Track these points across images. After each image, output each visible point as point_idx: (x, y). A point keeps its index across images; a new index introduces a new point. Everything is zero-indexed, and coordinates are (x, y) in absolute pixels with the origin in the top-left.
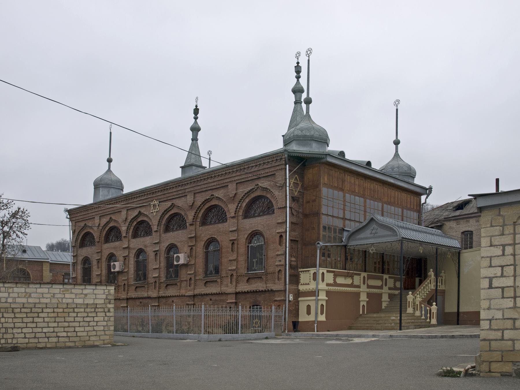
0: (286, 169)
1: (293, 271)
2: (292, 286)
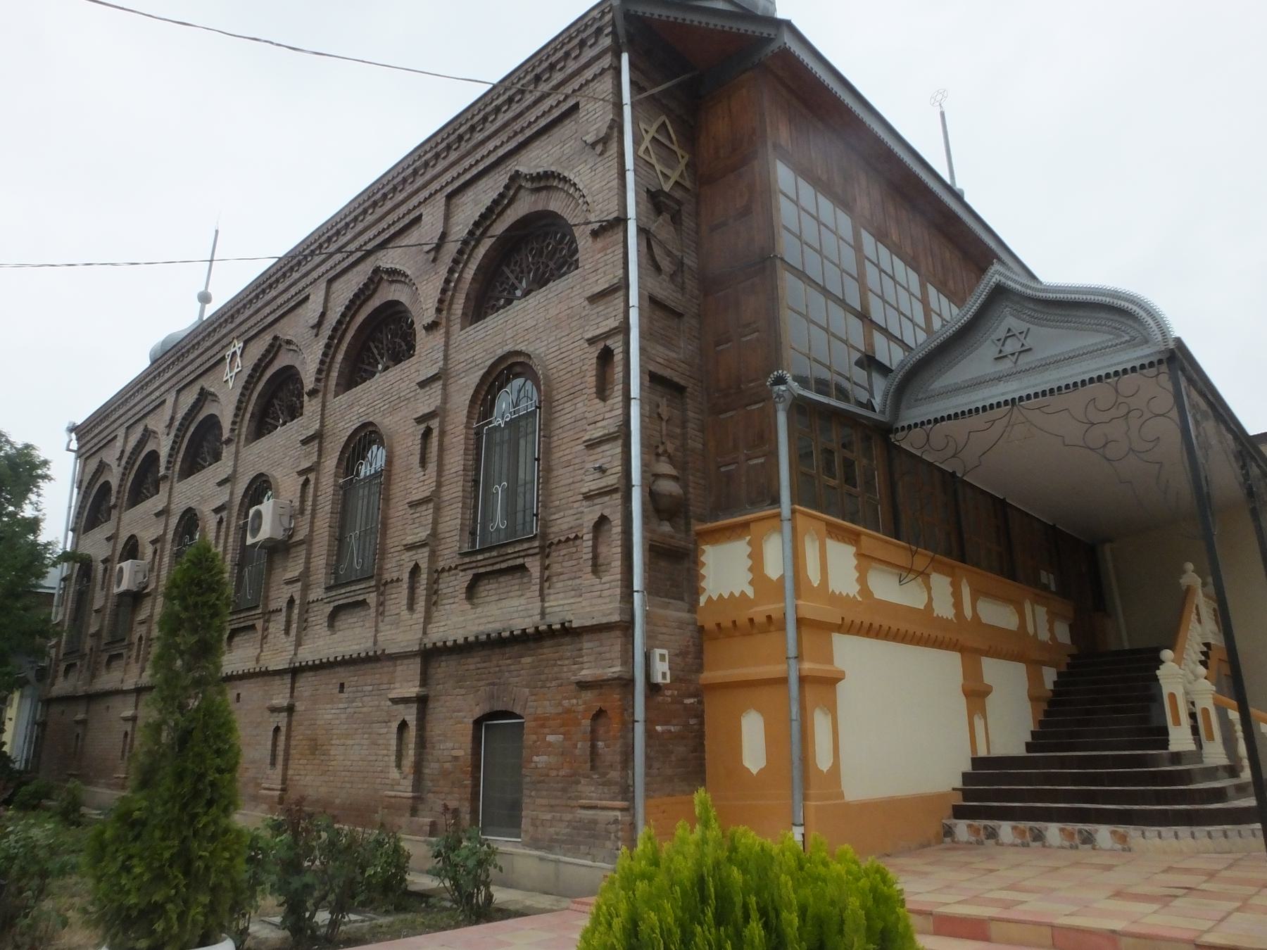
1: (666, 528)
2: (666, 606)
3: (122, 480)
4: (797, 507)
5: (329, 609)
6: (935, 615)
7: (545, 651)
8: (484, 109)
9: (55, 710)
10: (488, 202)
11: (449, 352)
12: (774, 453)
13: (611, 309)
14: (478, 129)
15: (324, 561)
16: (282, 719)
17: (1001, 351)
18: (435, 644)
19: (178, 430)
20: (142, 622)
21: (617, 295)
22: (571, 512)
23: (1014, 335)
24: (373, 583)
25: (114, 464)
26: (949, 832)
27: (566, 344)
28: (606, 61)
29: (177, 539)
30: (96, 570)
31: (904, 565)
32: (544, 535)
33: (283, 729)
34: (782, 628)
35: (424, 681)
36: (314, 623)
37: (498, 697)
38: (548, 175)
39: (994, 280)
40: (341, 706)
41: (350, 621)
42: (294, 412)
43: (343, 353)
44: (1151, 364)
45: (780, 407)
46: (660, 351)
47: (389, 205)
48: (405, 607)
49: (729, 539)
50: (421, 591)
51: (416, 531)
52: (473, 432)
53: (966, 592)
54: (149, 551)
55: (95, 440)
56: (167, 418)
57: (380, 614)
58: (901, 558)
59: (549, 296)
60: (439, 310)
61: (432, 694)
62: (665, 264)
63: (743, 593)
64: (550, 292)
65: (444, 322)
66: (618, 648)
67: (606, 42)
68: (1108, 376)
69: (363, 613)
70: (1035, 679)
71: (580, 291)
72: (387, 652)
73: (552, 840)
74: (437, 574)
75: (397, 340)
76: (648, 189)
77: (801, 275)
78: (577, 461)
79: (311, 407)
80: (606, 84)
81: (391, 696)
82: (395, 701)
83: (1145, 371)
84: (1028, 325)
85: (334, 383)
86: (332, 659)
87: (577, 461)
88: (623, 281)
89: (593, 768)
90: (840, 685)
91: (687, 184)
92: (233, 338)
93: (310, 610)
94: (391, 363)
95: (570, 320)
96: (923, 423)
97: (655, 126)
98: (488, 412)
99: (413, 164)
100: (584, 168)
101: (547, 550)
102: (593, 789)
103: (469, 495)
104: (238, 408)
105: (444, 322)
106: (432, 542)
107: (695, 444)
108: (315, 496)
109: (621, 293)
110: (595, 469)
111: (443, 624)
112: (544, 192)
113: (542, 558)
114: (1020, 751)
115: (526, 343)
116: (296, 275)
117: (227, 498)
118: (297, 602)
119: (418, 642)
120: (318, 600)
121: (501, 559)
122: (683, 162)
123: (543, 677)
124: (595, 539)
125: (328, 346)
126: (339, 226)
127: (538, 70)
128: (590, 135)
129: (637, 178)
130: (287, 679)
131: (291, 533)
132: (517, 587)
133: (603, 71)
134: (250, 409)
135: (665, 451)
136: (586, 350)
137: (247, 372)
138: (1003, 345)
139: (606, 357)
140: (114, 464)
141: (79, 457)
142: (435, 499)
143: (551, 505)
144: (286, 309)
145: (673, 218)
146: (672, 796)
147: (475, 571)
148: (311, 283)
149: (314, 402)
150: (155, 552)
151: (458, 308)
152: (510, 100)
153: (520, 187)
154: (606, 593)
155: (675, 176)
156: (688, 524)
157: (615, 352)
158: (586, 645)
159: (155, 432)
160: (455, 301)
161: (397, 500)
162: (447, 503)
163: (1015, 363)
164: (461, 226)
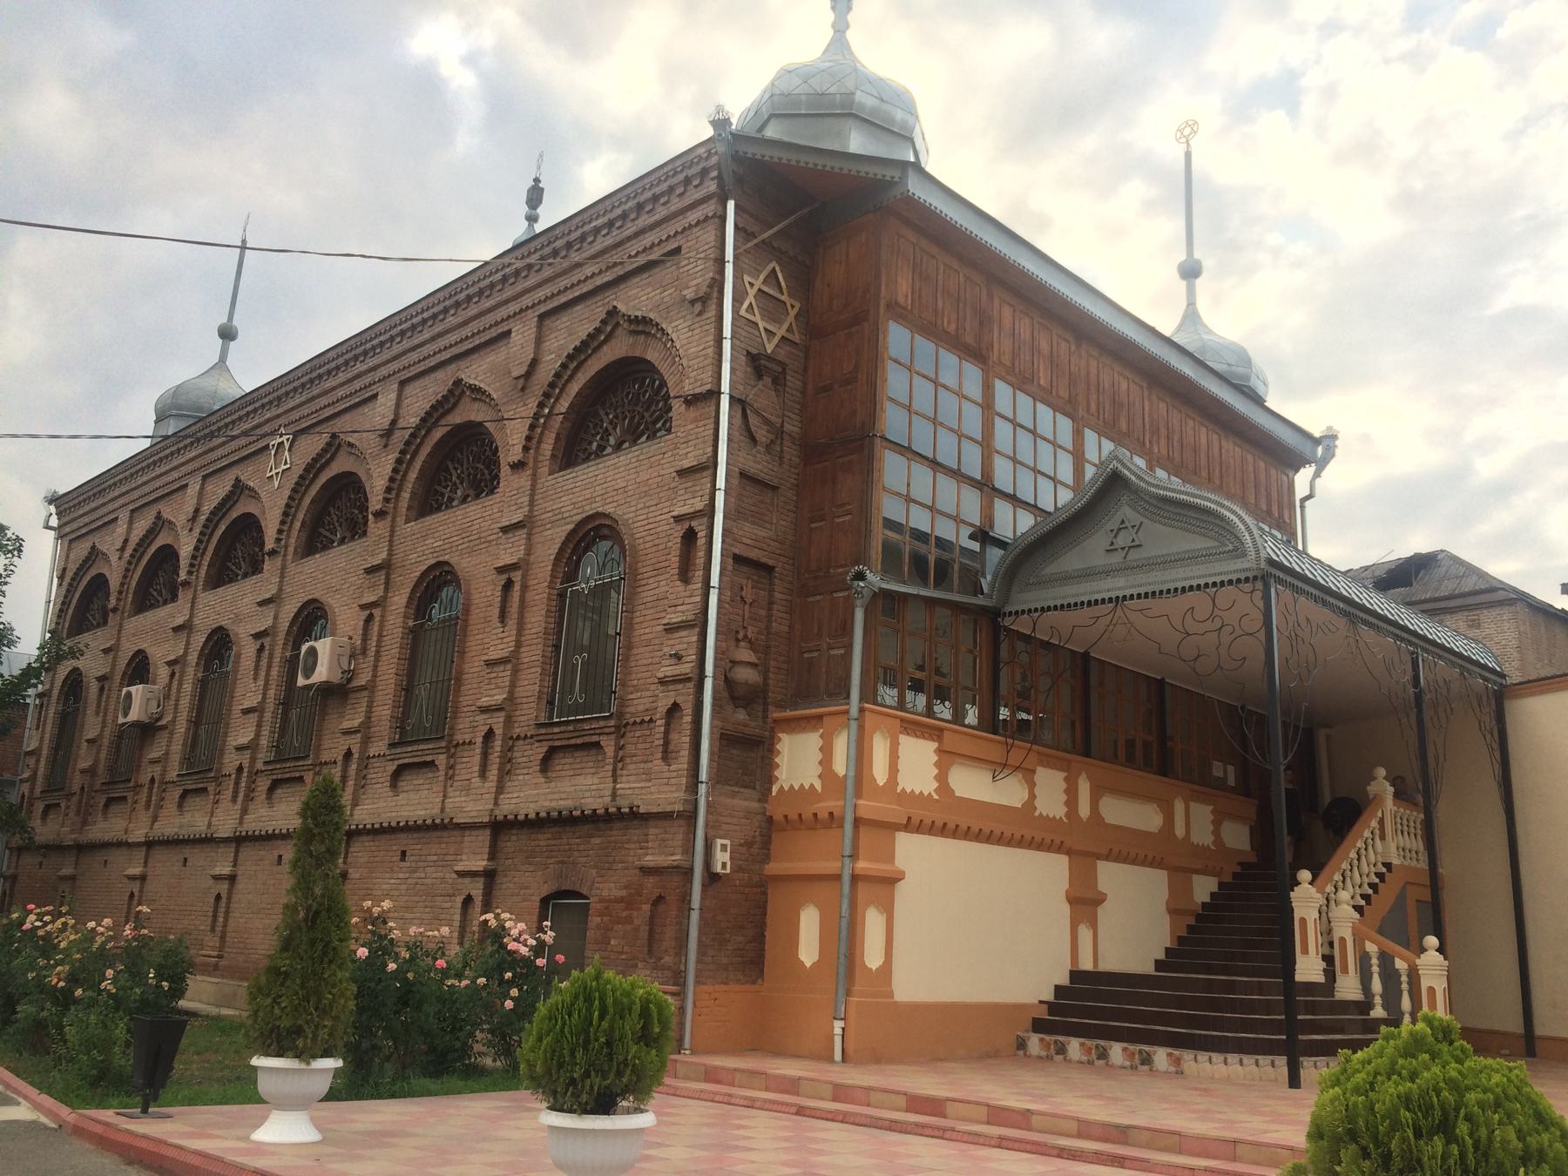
0: (723, 219)
1: (741, 715)
2: (734, 795)
3: (125, 577)
4: (866, 705)
5: (392, 767)
6: (1037, 814)
7: (614, 833)
8: (582, 226)
9: (28, 860)
10: (583, 335)
11: (536, 497)
12: (849, 647)
13: (698, 488)
14: (575, 248)
15: (389, 712)
17: (1112, 544)
18: (505, 816)
19: (205, 526)
20: (154, 762)
21: (704, 474)
22: (648, 694)
23: (1126, 528)
25: (114, 558)
26: (1022, 1045)
27: (655, 514)
28: (710, 208)
29: (203, 662)
30: (88, 688)
31: (999, 761)
32: (620, 715)
34: (841, 826)
35: (492, 856)
36: (373, 781)
37: (567, 876)
38: (645, 321)
39: (1111, 466)
40: (401, 876)
41: (415, 782)
42: (357, 529)
43: (416, 471)
44: (1247, 580)
45: (858, 602)
46: (748, 530)
47: (473, 310)
48: (476, 774)
49: (804, 730)
50: (495, 758)
51: (491, 692)
52: (556, 592)
54: (163, 673)
55: (86, 519)
56: (191, 509)
57: (450, 778)
59: (641, 458)
60: (526, 449)
61: (500, 868)
62: (762, 434)
63: (812, 784)
64: (642, 453)
65: (531, 465)
66: (680, 837)
67: (712, 187)
68: (1206, 585)
69: (430, 775)
70: (1179, 889)
71: (672, 459)
72: (454, 821)
74: (511, 741)
75: (480, 466)
76: (748, 352)
77: (907, 451)
78: (657, 641)
79: (377, 529)
80: (709, 235)
81: (456, 868)
82: (461, 874)
83: (1240, 586)
84: (1142, 519)
85: (406, 505)
87: (657, 641)
88: (711, 459)
89: (650, 952)
90: (900, 886)
91: (796, 338)
92: (280, 426)
93: (370, 766)
94: (471, 492)
95: (659, 490)
96: (1030, 610)
97: (762, 277)
98: (571, 576)
99: (502, 269)
100: (682, 325)
101: (623, 730)
102: (648, 973)
103: (548, 661)
104: (285, 514)
105: (531, 465)
106: (508, 707)
108: (380, 636)
110: (671, 655)
111: (516, 795)
112: (642, 337)
113: (617, 739)
114: (1149, 969)
115: (615, 504)
116: (360, 367)
117: (269, 622)
118: (356, 756)
119: (488, 813)
120: (379, 755)
121: (577, 734)
122: (793, 313)
123: (611, 859)
124: (668, 725)
125: (399, 461)
126: (415, 321)
127: (641, 199)
128: (690, 290)
129: (738, 342)
131: (350, 675)
132: (591, 764)
133: (707, 219)
134: (301, 516)
135: (746, 636)
136: (672, 526)
137: (298, 471)
138: (1115, 537)
139: (690, 537)
140: (114, 558)
141: (60, 537)
142: (514, 661)
143: (630, 683)
144: (348, 404)
145: (775, 381)
146: (726, 984)
147: (551, 743)
148: (379, 381)
149: (380, 524)
150: (173, 675)
151: (547, 447)
152: (610, 224)
153: (618, 324)
154: (673, 781)
155: (781, 331)
156: (765, 711)
157: (699, 535)
158: (652, 831)
159: (170, 523)
160: (545, 439)
161: (474, 653)
162: (526, 666)
163: (1125, 558)
164: (553, 356)
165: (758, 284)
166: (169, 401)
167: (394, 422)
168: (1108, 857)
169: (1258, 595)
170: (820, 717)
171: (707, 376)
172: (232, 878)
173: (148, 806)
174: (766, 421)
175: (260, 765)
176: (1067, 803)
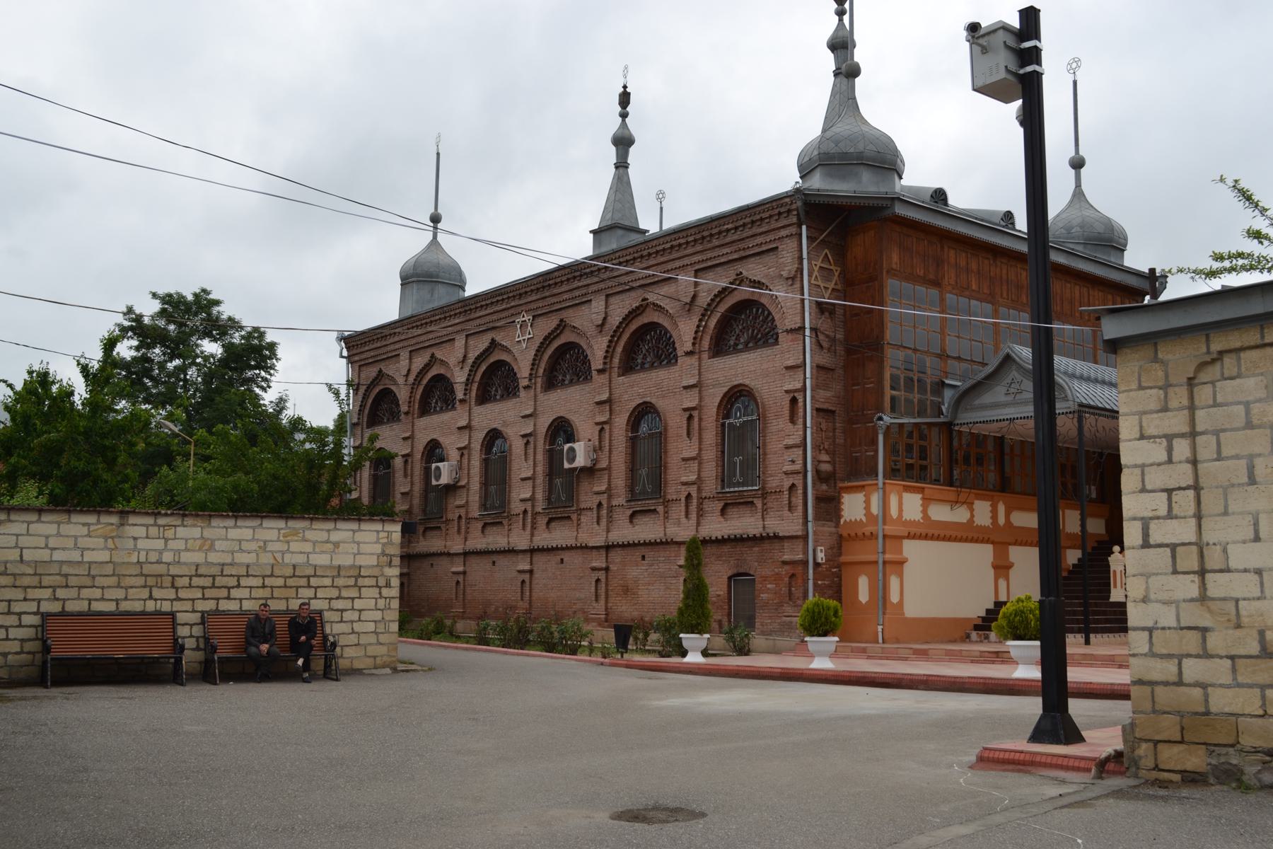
1: (824, 487)
2: (823, 525)
4: (887, 481)
12: (876, 451)
16: (602, 575)
24: (661, 500)
25: (401, 380)
26: (968, 636)
28: (793, 230)
32: (763, 488)
33: (603, 580)
34: (877, 538)
44: (1070, 412)
45: (880, 431)
46: (823, 394)
49: (855, 492)
53: (1001, 509)
55: (372, 354)
56: (461, 356)
57: (666, 518)
58: (952, 496)
60: (694, 344)
62: (825, 344)
66: (801, 547)
73: (771, 631)
79: (599, 380)
86: (636, 542)
89: (790, 599)
90: (905, 565)
91: (839, 287)
97: (820, 260)
104: (533, 364)
106: (699, 482)
107: (840, 441)
109: (802, 368)
122: (837, 274)
124: (790, 493)
125: (610, 341)
130: (603, 552)
131: (595, 461)
139: (794, 401)
140: (401, 380)
145: (830, 314)
156: (835, 483)
158: (786, 544)
165: (819, 264)
166: (411, 272)
167: (605, 319)
168: (1015, 544)
169: (1076, 420)
170: (863, 486)
171: (798, 319)
172: (531, 572)
173: (459, 532)
174: (827, 336)
175: (539, 509)
176: (992, 518)
